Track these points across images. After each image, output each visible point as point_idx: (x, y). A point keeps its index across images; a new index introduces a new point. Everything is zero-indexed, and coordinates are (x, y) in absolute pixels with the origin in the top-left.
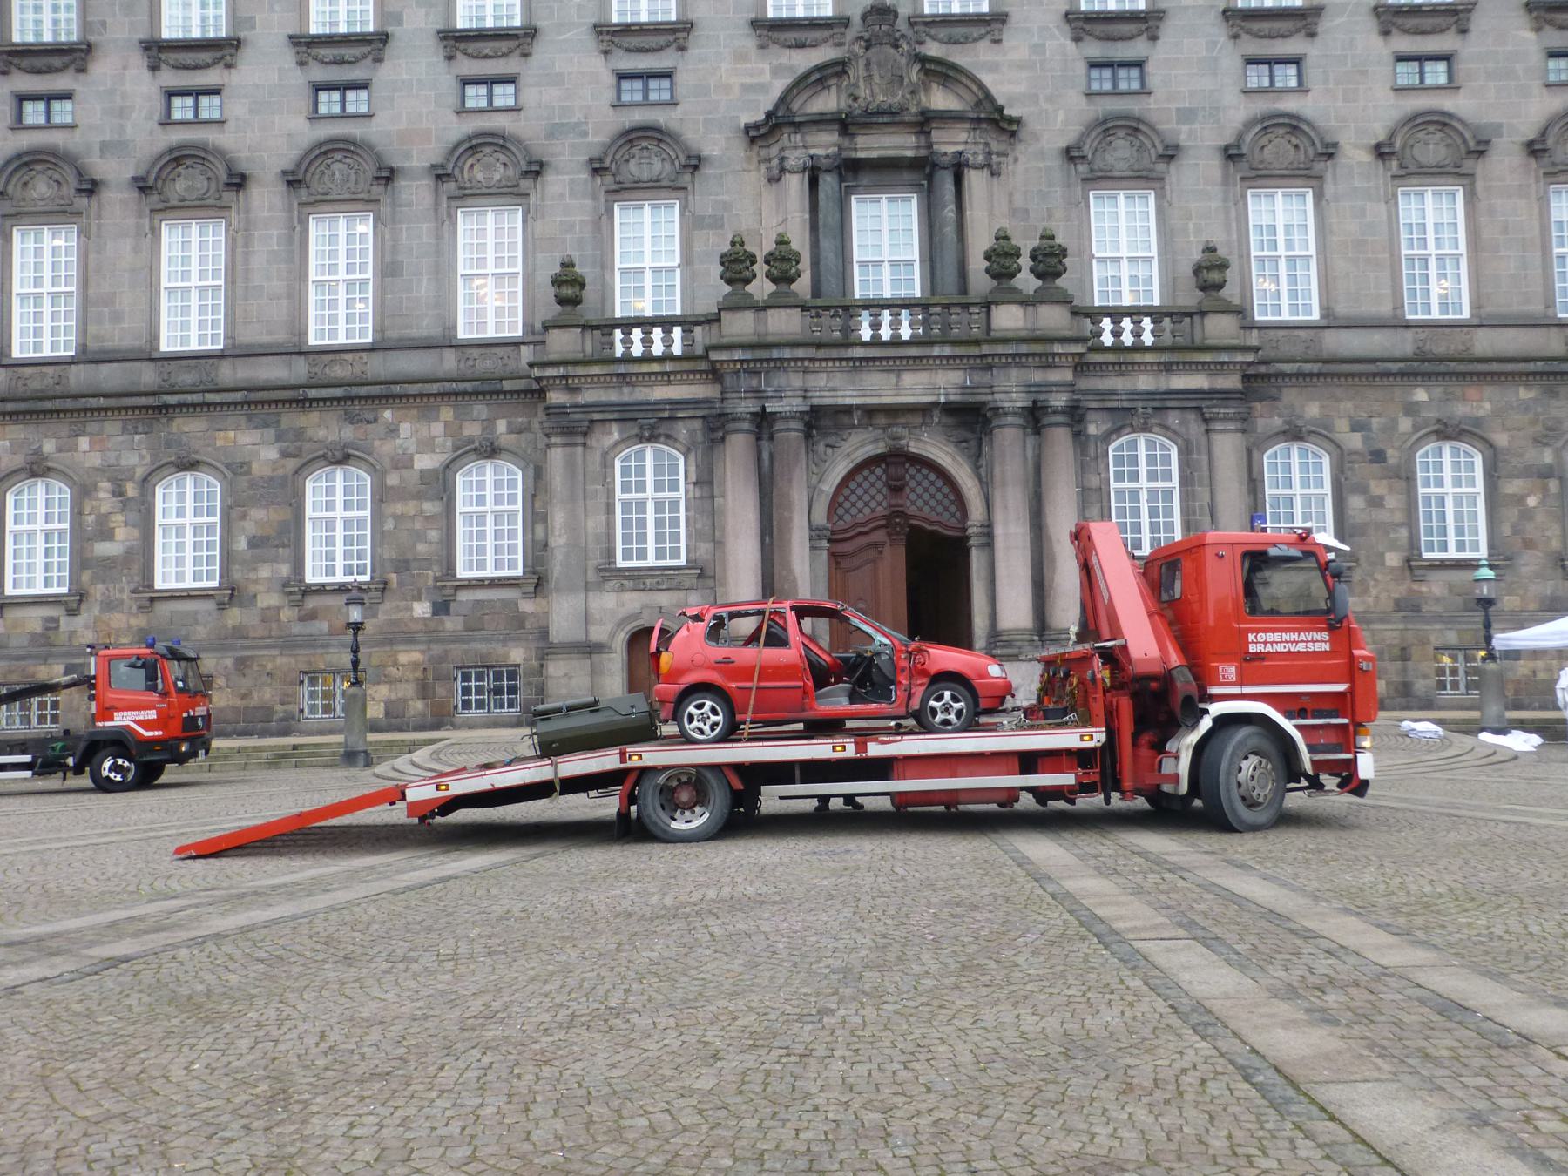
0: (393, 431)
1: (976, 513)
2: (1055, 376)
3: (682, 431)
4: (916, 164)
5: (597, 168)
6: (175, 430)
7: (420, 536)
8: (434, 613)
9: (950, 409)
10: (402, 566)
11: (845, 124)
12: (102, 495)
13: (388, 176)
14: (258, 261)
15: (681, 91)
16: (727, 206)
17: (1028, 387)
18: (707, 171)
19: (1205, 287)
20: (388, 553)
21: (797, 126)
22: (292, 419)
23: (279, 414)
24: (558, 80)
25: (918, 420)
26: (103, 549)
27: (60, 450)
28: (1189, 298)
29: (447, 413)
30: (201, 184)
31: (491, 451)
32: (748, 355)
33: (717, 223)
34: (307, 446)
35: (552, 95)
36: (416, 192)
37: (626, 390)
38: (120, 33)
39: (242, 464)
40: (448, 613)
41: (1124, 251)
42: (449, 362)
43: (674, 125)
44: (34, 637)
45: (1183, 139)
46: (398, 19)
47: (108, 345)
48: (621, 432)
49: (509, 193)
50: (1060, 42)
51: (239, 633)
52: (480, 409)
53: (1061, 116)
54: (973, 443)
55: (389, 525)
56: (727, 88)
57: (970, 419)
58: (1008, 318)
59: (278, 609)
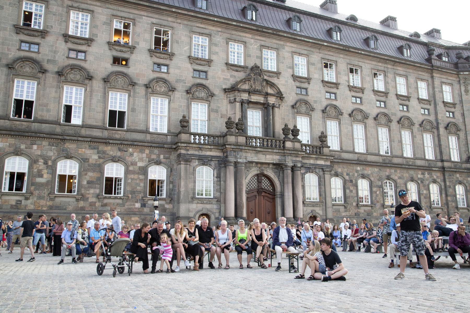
0: (132, 155)
2: (298, 159)
3: (213, 163)
4: (263, 104)
5: (188, 92)
6: (66, 147)
7: (138, 185)
8: (141, 207)
9: (274, 164)
10: (133, 192)
12: (40, 163)
13: (133, 84)
14: (94, 101)
15: (209, 77)
16: (219, 107)
17: (293, 161)
18: (214, 98)
20: (128, 189)
21: (239, 91)
22: (102, 147)
23: (99, 146)
24: (179, 68)
25: (267, 166)
26: (39, 180)
27: (26, 148)
28: (318, 143)
29: (147, 151)
30: (78, 77)
31: (158, 163)
32: (235, 147)
33: (217, 111)
34: (106, 156)
35: (177, 71)
36: (141, 91)
37: (200, 151)
39: (86, 159)
40: (145, 207)
42: (148, 137)
43: (207, 85)
44: (12, 206)
45: (315, 107)
46: (138, 43)
47: (45, 118)
48: (198, 162)
49: (165, 94)
50: (291, 80)
51: (83, 208)
52: (156, 151)
53: (291, 98)
54: (278, 173)
55: (130, 181)
56: (220, 78)
57: (279, 167)
59: (95, 202)
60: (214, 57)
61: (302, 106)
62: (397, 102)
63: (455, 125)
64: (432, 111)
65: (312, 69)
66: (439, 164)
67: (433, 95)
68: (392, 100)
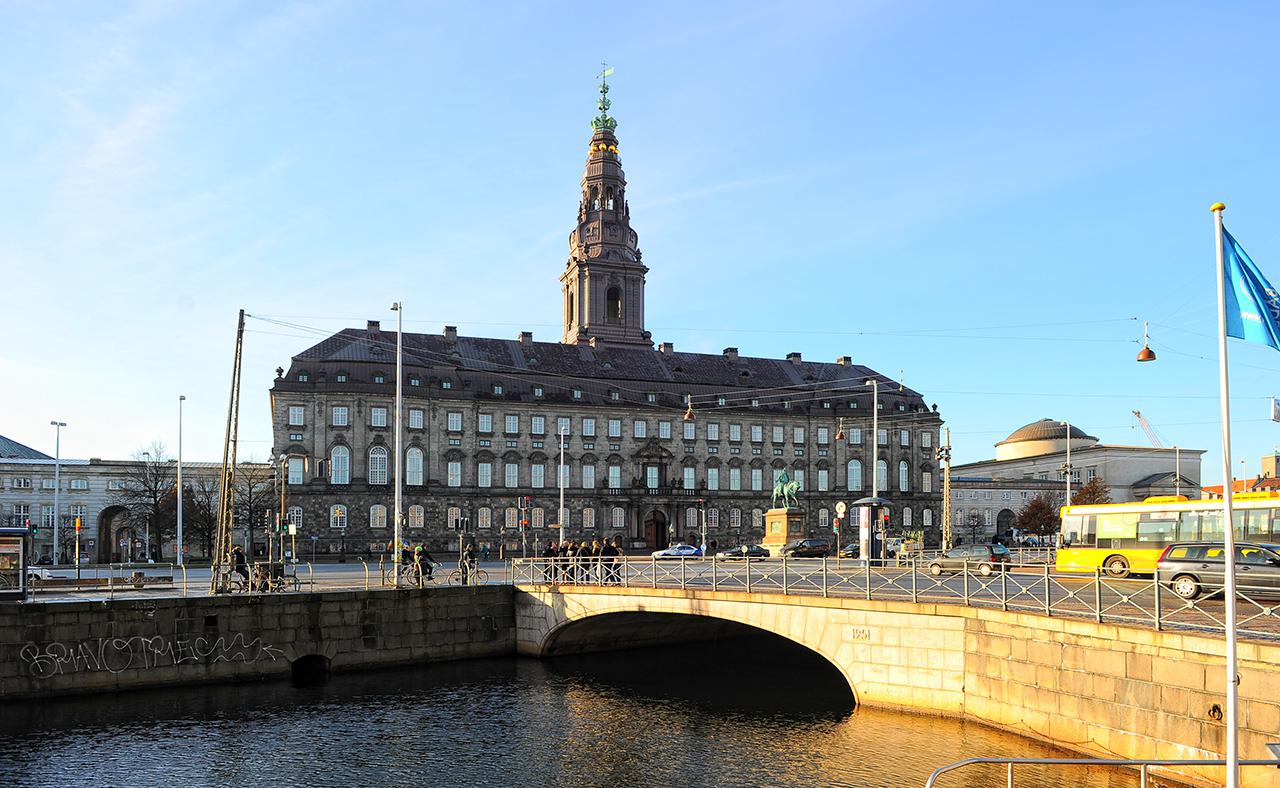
1: (667, 519)
11: (648, 457)
19: (703, 486)
28: (699, 487)
31: (589, 506)
35: (600, 448)
38: (526, 431)
41: (689, 478)
42: (583, 492)
52: (588, 500)
58: (675, 492)
60: (624, 434)
61: (690, 461)
62: (772, 448)
63: (826, 462)
64: (806, 451)
65: (698, 432)
66: (807, 494)
67: (807, 439)
68: (768, 446)
